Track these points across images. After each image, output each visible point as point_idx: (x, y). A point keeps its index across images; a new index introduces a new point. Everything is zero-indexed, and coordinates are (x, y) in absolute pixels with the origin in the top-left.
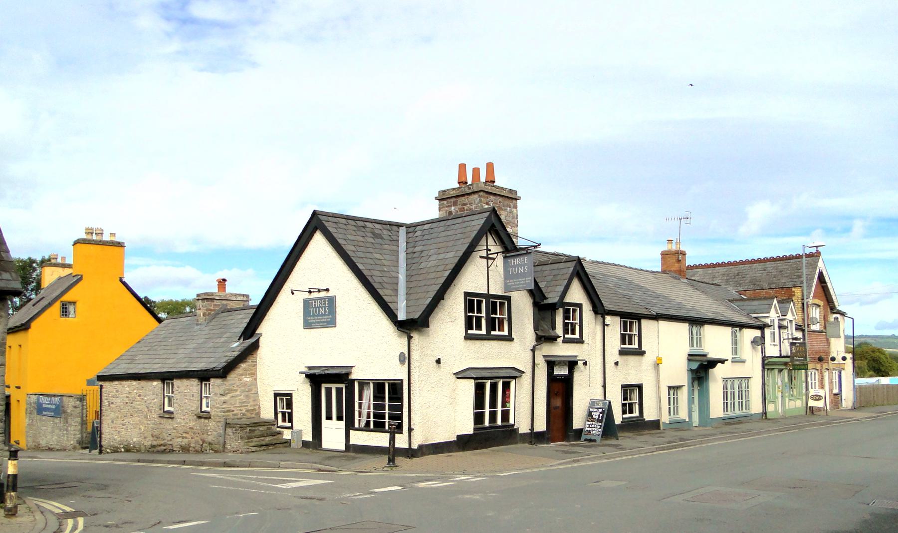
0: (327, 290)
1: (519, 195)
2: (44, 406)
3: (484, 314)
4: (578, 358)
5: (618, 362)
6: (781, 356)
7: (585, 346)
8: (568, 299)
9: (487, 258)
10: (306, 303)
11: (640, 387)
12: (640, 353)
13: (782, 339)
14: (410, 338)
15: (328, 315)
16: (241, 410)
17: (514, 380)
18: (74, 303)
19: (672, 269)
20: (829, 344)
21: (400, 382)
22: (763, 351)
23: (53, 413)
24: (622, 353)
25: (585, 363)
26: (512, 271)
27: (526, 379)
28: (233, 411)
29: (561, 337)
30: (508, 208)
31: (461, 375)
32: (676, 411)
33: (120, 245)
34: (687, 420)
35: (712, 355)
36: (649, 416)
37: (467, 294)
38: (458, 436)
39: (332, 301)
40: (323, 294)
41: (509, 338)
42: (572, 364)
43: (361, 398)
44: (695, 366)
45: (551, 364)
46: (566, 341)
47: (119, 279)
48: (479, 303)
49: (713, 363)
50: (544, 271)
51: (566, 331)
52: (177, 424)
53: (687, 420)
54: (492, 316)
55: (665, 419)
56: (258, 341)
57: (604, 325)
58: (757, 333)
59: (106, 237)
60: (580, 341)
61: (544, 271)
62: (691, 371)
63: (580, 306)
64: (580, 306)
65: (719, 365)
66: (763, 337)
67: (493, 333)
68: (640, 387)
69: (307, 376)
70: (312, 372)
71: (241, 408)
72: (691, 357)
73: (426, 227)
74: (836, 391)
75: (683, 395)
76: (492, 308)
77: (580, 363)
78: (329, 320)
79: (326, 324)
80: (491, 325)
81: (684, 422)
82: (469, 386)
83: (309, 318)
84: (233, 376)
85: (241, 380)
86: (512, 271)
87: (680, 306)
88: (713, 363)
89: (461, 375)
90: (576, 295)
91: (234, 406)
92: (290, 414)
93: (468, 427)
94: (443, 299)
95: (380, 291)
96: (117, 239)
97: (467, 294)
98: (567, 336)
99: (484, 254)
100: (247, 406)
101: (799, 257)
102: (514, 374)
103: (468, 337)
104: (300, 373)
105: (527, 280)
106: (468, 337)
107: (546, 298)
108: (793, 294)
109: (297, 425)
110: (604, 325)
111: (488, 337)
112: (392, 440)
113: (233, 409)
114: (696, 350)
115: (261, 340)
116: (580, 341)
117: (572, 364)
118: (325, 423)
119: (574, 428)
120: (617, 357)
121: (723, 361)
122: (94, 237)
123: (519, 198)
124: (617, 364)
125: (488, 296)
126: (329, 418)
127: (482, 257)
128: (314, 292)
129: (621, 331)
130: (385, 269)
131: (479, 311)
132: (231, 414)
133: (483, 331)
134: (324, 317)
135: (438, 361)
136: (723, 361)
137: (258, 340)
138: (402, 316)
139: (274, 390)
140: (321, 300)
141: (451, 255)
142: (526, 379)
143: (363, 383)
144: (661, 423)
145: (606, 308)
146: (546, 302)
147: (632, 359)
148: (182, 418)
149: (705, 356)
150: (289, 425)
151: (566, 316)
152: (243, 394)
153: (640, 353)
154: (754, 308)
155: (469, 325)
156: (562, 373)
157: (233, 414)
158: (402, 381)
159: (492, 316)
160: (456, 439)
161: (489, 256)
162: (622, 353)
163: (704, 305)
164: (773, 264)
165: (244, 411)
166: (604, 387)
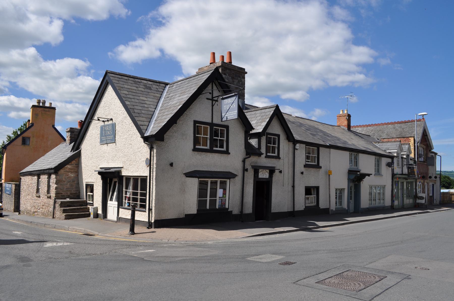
0: (112, 119)
1: (246, 71)
2: (7, 189)
3: (208, 136)
4: (276, 168)
5: (303, 172)
6: (402, 174)
7: (281, 161)
8: (269, 131)
9: (212, 100)
10: (102, 128)
11: (317, 188)
12: (318, 166)
13: (403, 165)
14: (151, 149)
15: (111, 135)
16: (67, 193)
17: (229, 180)
18: (29, 138)
19: (343, 124)
20: (428, 169)
21: (145, 178)
22: (393, 170)
23: (9, 193)
24: (306, 166)
25: (281, 172)
26: (226, 107)
27: (238, 180)
28: (62, 193)
29: (263, 154)
30: (239, 78)
31: (190, 175)
32: (341, 203)
33: (54, 109)
34: (347, 209)
35: (363, 171)
36: (322, 205)
37: (195, 122)
38: (186, 215)
39: (114, 126)
40: (110, 122)
41: (227, 152)
42: (272, 171)
43: (127, 188)
44: (353, 177)
45: (256, 170)
46: (267, 157)
47: (52, 126)
48: (205, 129)
49: (363, 176)
50: (256, 114)
51: (267, 151)
52: (41, 200)
53: (347, 209)
54: (214, 138)
55: (333, 207)
56: (80, 151)
57: (295, 149)
58: (389, 160)
59: (47, 105)
60: (278, 157)
61: (256, 114)
62: (349, 179)
63: (278, 136)
64: (278, 136)
65: (367, 177)
66: (393, 162)
67: (215, 149)
68: (317, 188)
69: (100, 173)
70: (103, 170)
71: (67, 192)
72: (350, 172)
73: (179, 83)
74: (431, 195)
75: (346, 194)
76: (214, 133)
77: (277, 171)
78: (112, 138)
79: (110, 141)
80: (213, 142)
81: (345, 209)
82: (194, 183)
83: (102, 138)
84: (62, 171)
85: (68, 175)
86: (226, 107)
87: (345, 142)
88: (363, 176)
89: (190, 175)
90: (276, 129)
91: (63, 190)
92: (93, 196)
93: (193, 209)
94: (176, 123)
95: (137, 119)
96: (53, 106)
97: (195, 122)
98: (268, 154)
99: (210, 97)
100: (72, 191)
101: (413, 121)
102: (230, 176)
103: (195, 150)
104: (95, 171)
105: (235, 113)
106: (195, 150)
107: (254, 129)
108: (410, 140)
109: (95, 205)
110: (295, 149)
111: (211, 151)
112: (133, 215)
113: (61, 192)
114: (354, 168)
115: (82, 151)
116: (278, 157)
117: (272, 171)
118: (109, 202)
119: (272, 212)
120: (303, 169)
121: (369, 175)
122: (41, 105)
123: (246, 73)
124: (302, 173)
125: (212, 125)
126: (111, 200)
127: (207, 99)
128: (105, 121)
129: (306, 153)
130: (146, 106)
131: (205, 134)
132: (60, 195)
133: (208, 147)
134: (109, 137)
135: (171, 165)
136: (369, 175)
137: (81, 150)
138: (147, 134)
139: (86, 182)
140: (108, 126)
141: (186, 96)
142: (238, 180)
143: (128, 178)
144: (330, 211)
145: (295, 139)
146: (253, 132)
147: (313, 170)
148: (42, 197)
149: (359, 172)
150: (92, 202)
151: (268, 141)
152: (69, 184)
153: (318, 166)
154: (389, 147)
155: (196, 141)
156: (264, 177)
157: (61, 196)
158: (147, 177)
159: (214, 138)
160: (184, 217)
161: (214, 99)
162: (306, 166)
163: (360, 144)
164: (399, 125)
165: (69, 194)
166: (293, 187)
